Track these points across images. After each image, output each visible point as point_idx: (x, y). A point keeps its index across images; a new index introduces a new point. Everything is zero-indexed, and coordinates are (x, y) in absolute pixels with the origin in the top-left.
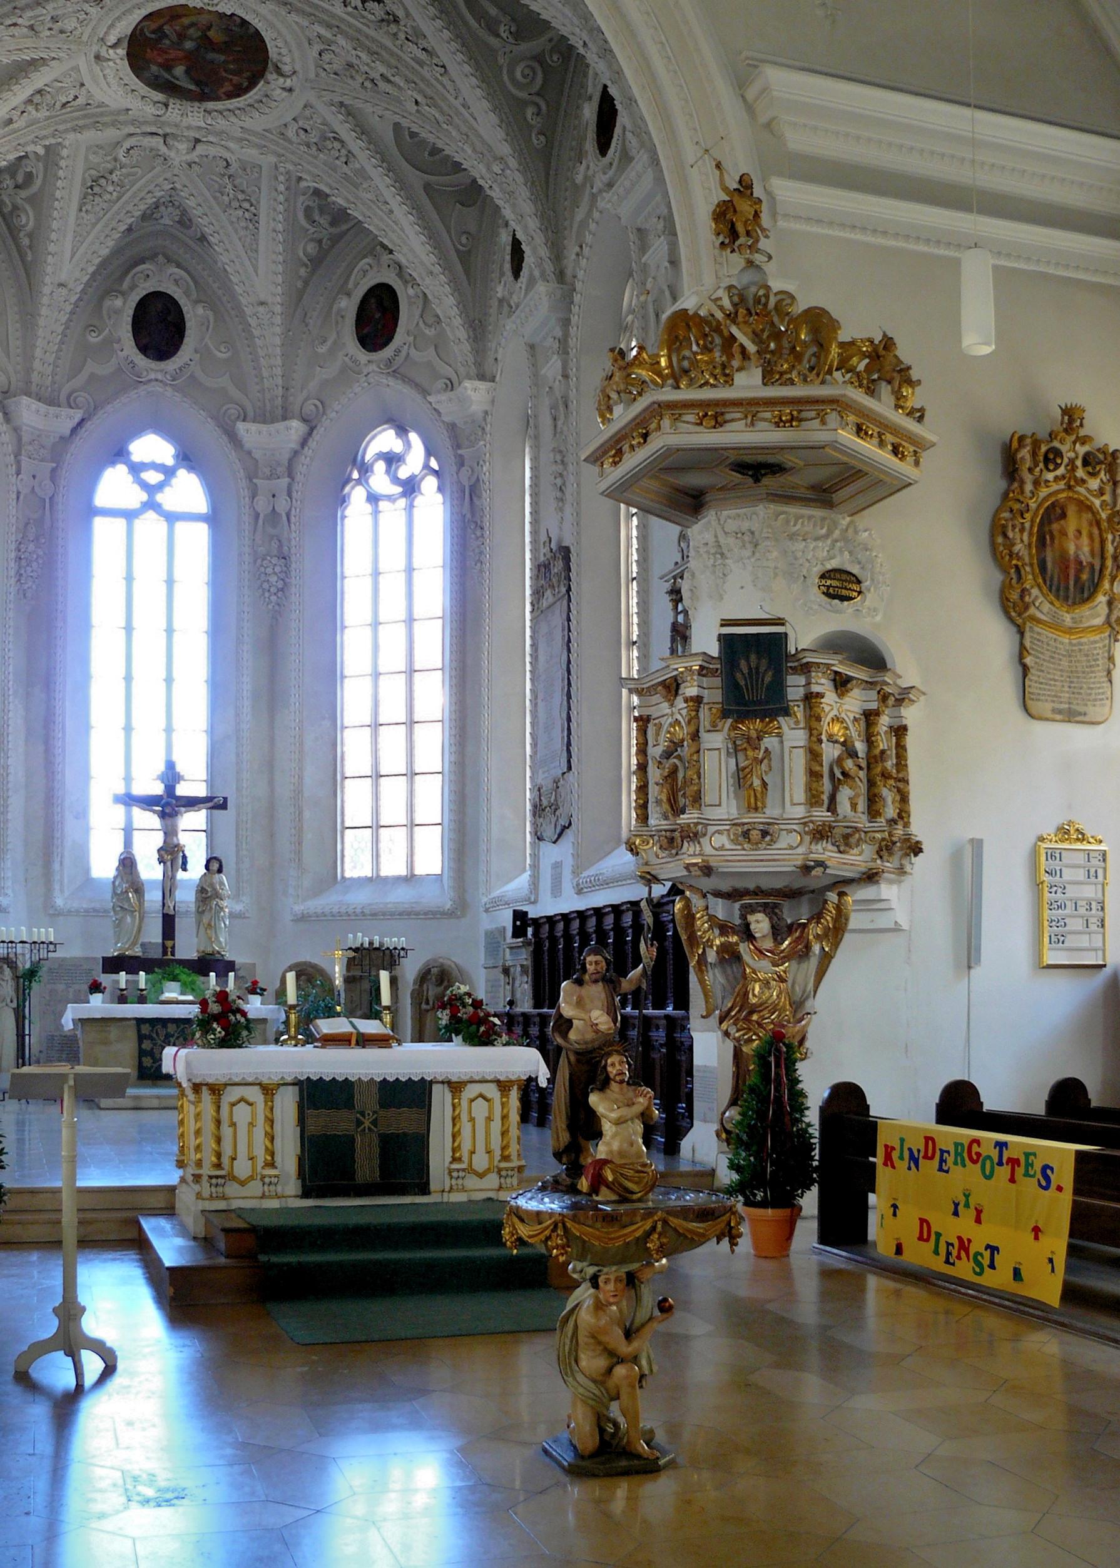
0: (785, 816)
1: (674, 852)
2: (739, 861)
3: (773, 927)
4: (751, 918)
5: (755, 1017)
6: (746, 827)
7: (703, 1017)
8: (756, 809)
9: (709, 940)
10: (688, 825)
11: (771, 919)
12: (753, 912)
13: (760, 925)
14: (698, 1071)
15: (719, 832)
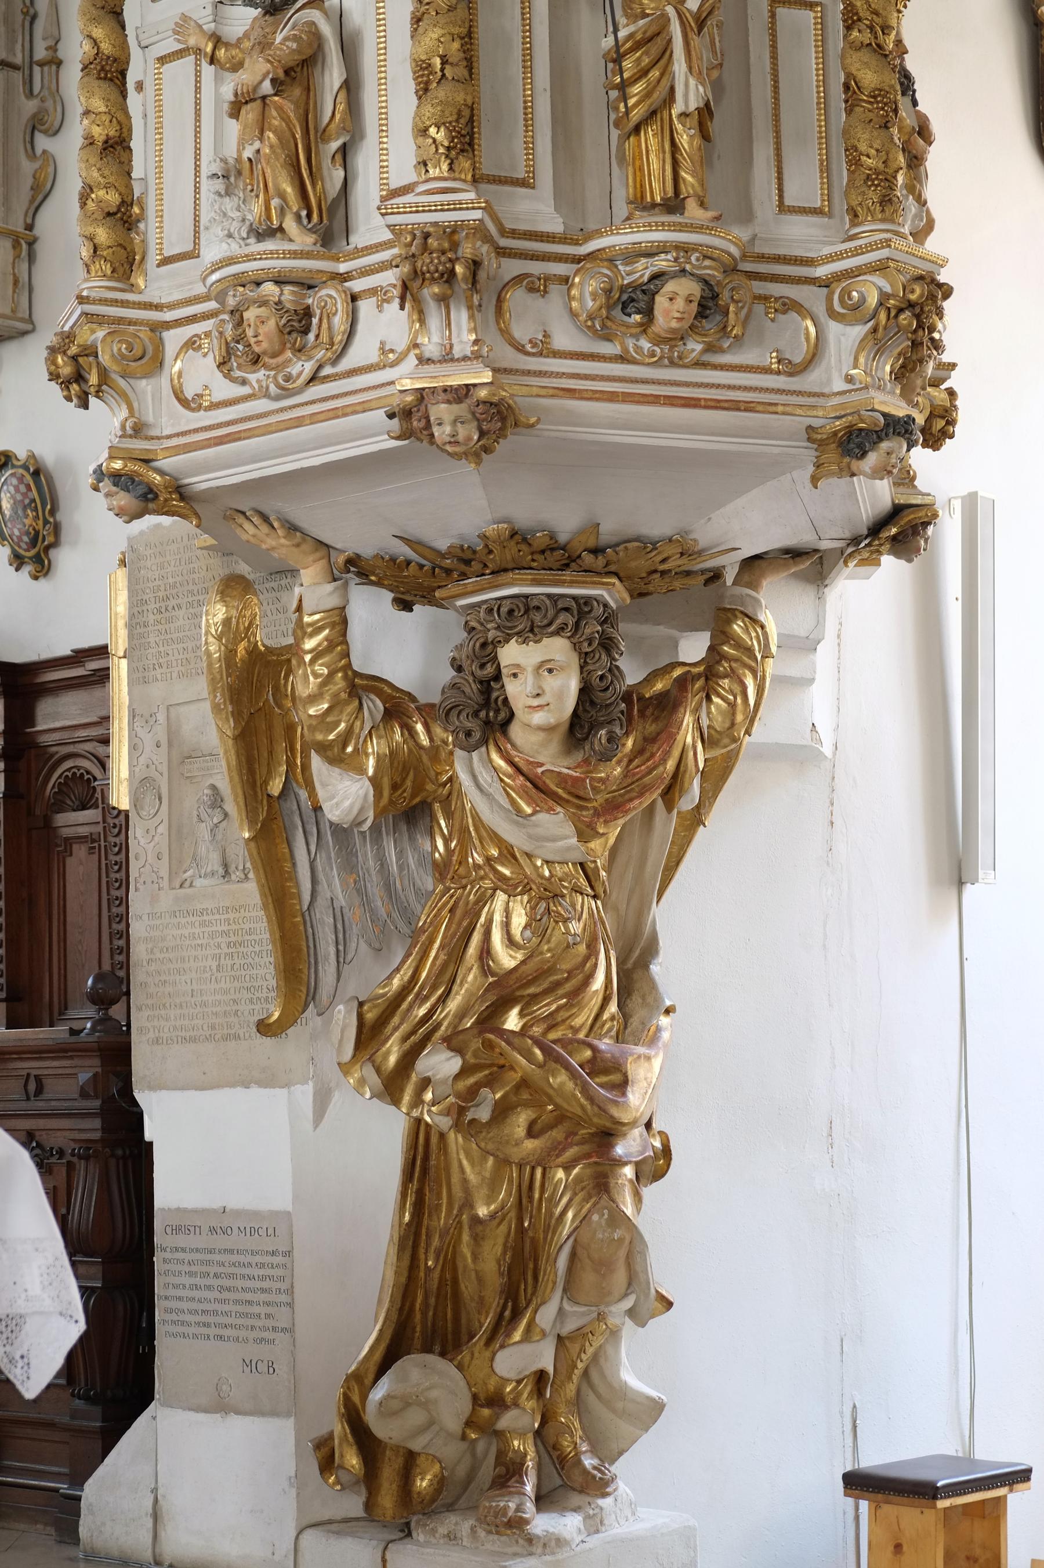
0: (759, 249)
1: (302, 368)
2: (612, 397)
3: (585, 691)
4: (511, 654)
5: (513, 1021)
6: (642, 270)
7: (264, 1028)
8: (674, 205)
9: (345, 739)
10: (452, 233)
11: (585, 660)
12: (532, 633)
13: (551, 683)
14: (178, 1230)
15: (537, 287)
